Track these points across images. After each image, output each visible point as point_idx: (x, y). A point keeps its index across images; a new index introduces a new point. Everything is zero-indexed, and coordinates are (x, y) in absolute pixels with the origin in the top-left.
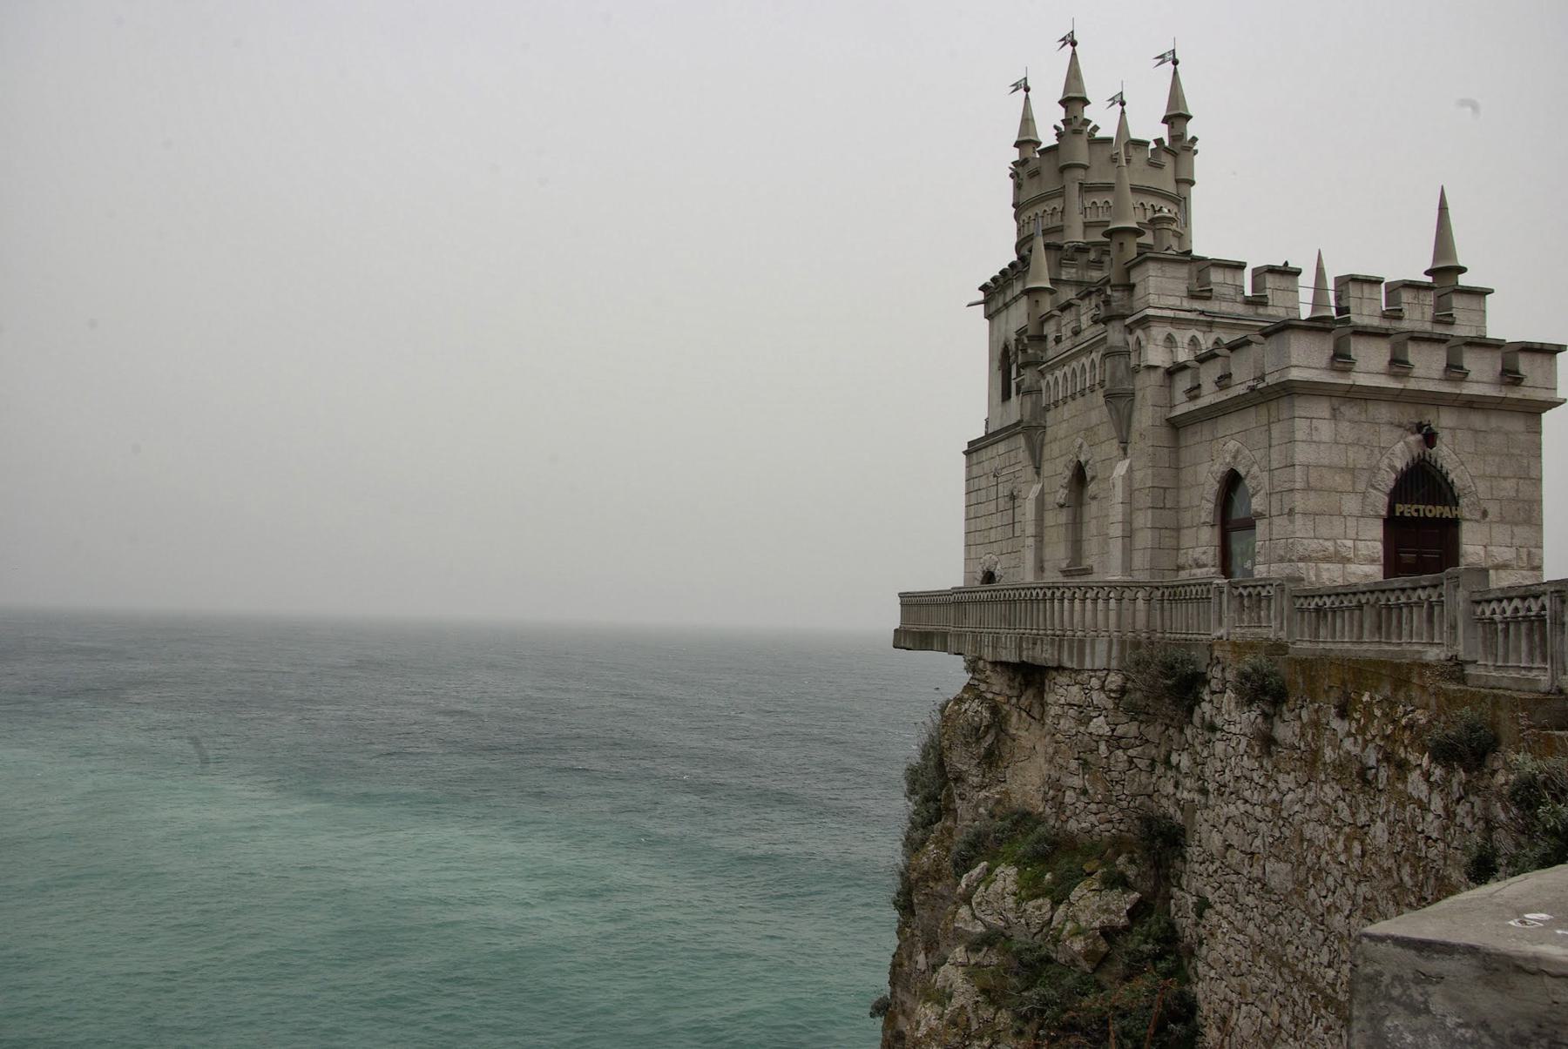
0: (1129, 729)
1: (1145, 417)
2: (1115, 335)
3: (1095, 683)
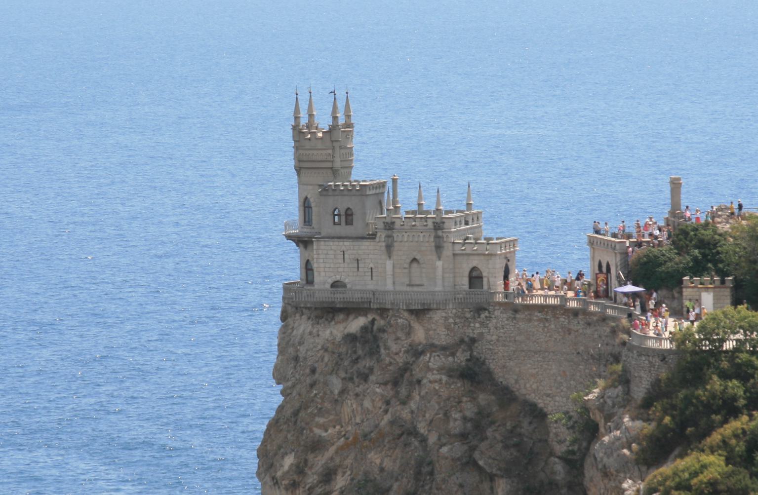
0: (457, 320)
1: (447, 252)
2: (440, 233)
3: (449, 312)
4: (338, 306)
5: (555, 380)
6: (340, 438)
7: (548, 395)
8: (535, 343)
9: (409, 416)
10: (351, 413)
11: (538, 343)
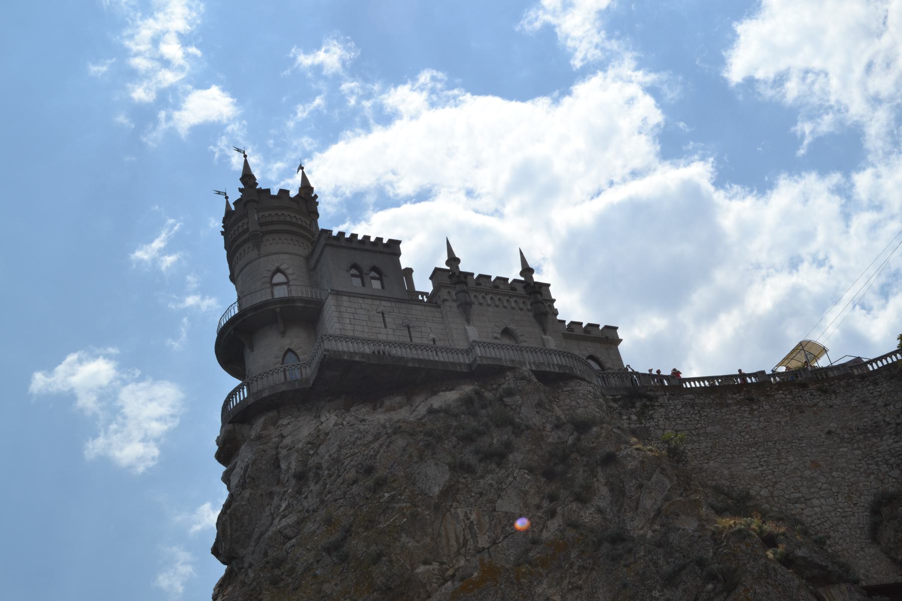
4: (410, 365)
5: (801, 477)
6: (443, 584)
7: (797, 501)
8: (743, 434)
9: (598, 516)
10: (467, 531)
11: (747, 433)
